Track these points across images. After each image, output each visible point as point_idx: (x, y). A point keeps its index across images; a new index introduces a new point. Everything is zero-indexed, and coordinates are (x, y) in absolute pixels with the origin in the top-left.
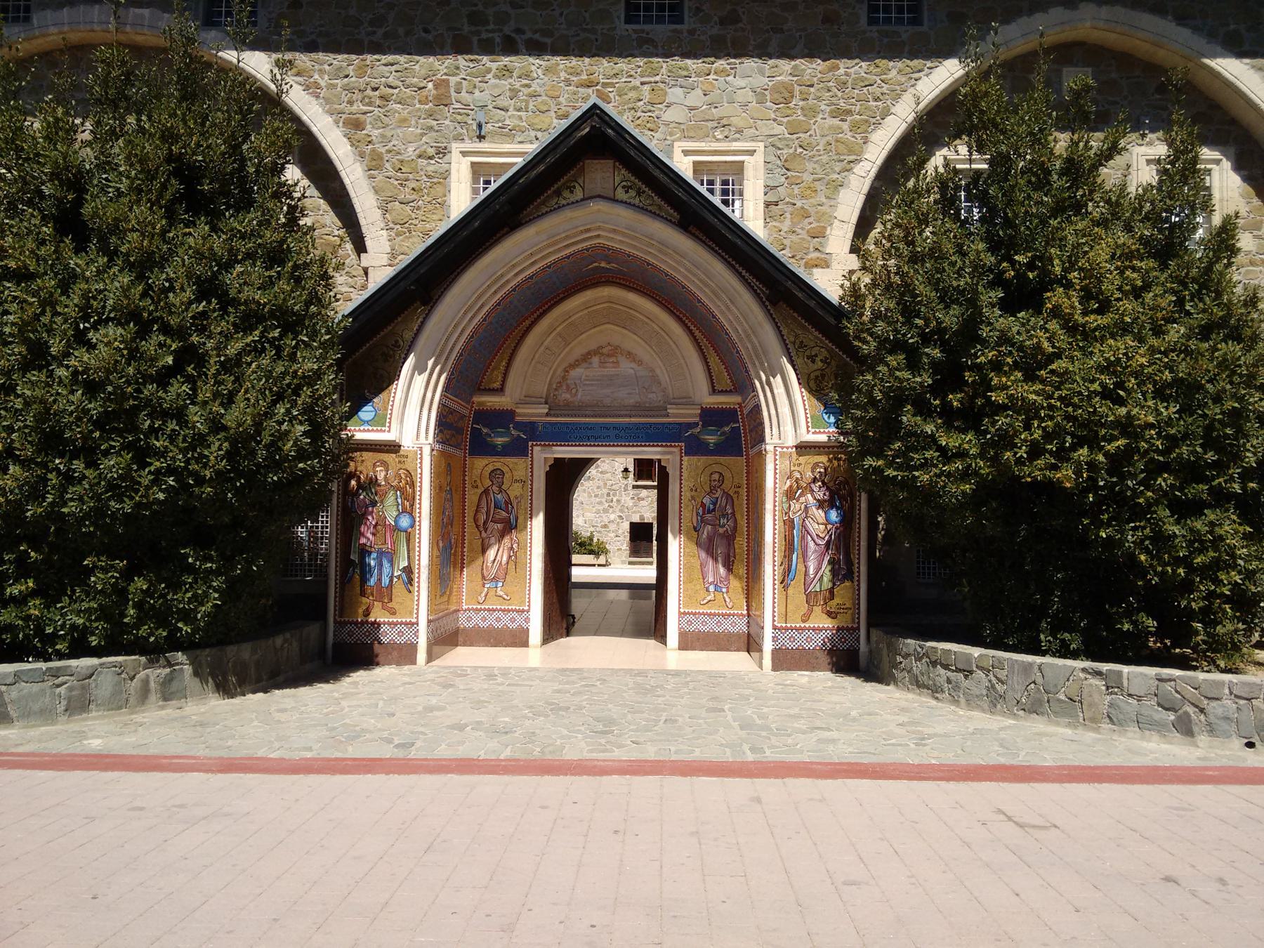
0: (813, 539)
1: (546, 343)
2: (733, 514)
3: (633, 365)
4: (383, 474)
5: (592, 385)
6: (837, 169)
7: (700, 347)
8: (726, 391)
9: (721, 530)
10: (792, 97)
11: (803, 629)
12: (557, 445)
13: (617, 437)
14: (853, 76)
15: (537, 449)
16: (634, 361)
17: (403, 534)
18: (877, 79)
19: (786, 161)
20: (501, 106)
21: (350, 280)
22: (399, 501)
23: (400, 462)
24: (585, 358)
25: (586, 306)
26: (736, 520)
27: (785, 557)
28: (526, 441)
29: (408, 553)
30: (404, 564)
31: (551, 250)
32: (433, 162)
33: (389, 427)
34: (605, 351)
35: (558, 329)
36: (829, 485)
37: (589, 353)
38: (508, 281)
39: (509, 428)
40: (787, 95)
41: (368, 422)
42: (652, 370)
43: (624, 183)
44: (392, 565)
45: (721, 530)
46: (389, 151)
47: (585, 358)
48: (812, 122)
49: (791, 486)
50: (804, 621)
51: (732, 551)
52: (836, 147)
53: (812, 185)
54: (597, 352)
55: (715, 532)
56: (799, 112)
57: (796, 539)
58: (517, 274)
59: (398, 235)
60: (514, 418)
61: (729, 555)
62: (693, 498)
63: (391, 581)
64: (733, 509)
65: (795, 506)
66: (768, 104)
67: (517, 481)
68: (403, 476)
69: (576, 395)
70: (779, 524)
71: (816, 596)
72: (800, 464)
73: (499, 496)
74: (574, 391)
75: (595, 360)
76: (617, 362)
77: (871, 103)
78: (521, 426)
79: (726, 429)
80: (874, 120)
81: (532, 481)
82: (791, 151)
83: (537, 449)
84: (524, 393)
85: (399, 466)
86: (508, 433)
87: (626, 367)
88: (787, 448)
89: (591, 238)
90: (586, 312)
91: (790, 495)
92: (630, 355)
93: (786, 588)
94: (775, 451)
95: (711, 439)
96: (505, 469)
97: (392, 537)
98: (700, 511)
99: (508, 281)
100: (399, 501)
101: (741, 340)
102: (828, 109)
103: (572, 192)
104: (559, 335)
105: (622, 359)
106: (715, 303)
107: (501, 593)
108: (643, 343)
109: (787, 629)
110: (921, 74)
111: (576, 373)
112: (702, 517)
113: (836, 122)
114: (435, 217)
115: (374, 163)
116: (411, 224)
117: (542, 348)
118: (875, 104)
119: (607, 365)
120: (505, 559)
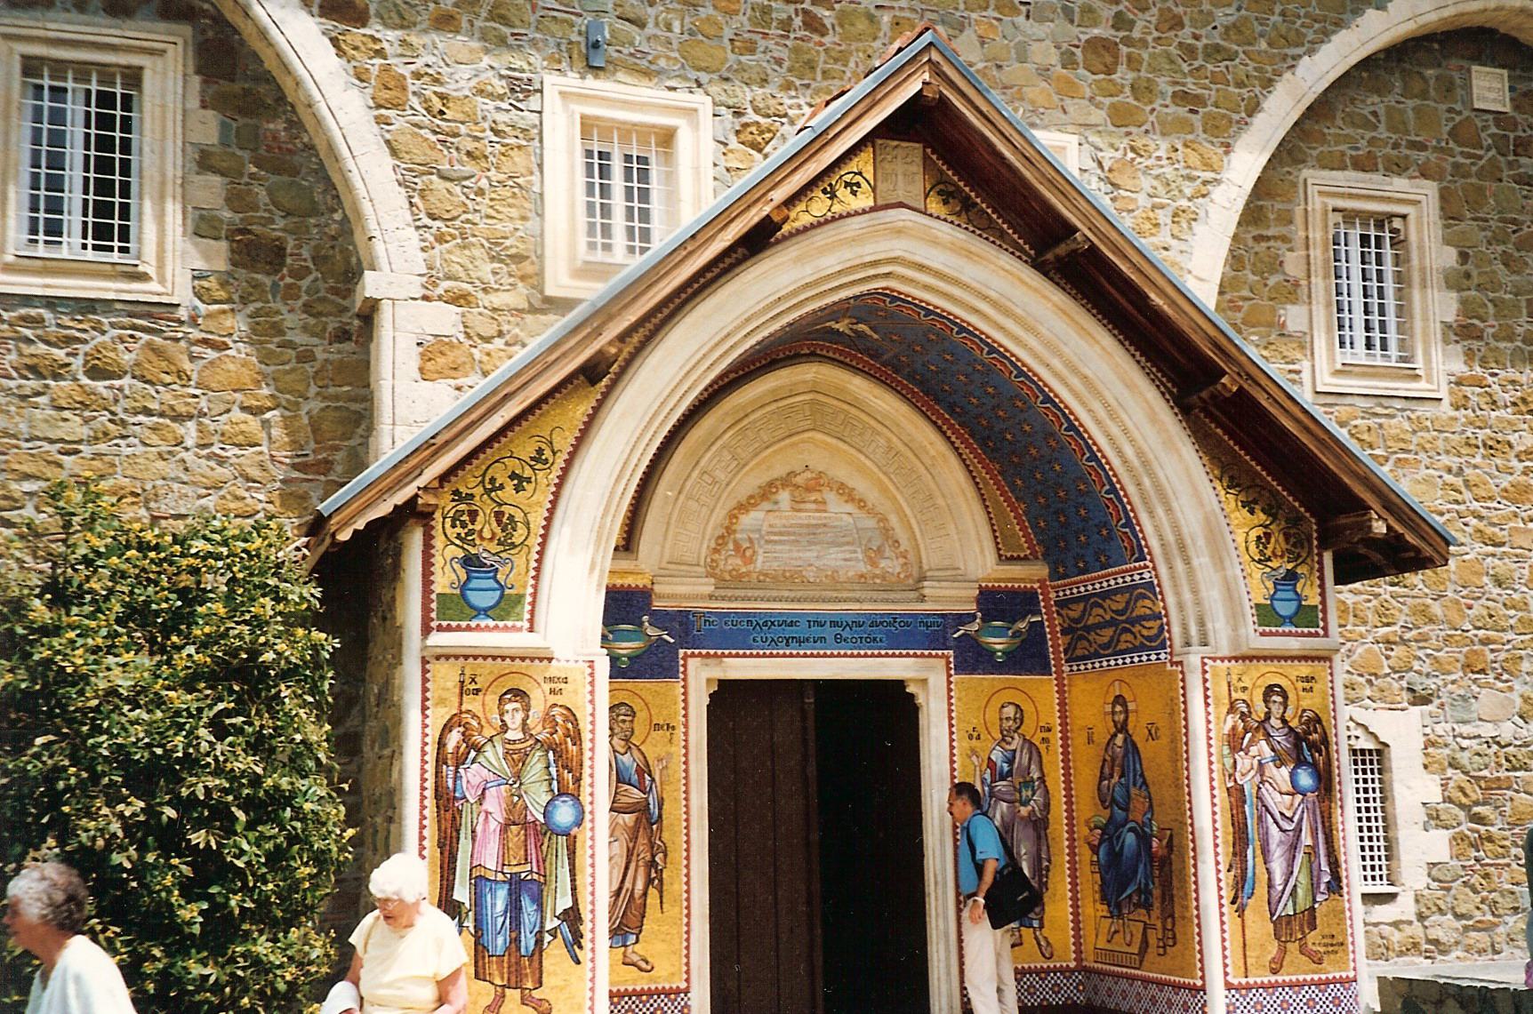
0: (1276, 822)
1: (703, 463)
2: (1042, 779)
3: (849, 508)
4: (520, 716)
5: (780, 542)
6: (1188, 192)
9: (1024, 811)
10: (1116, 63)
11: (1274, 986)
12: (730, 656)
13: (839, 639)
14: (1205, 41)
15: (693, 664)
16: (853, 500)
17: (562, 840)
18: (1240, 49)
19: (1110, 170)
20: (631, 16)
21: (312, 321)
22: (553, 770)
23: (552, 692)
24: (766, 493)
26: (1047, 792)
27: (1235, 854)
28: (673, 650)
29: (573, 880)
30: (565, 903)
31: (809, 294)
32: (505, 106)
33: (531, 621)
34: (799, 480)
36: (1295, 723)
37: (771, 484)
39: (641, 624)
40: (1109, 59)
41: (486, 612)
42: (884, 519)
43: (942, 187)
44: (541, 908)
45: (1024, 811)
46: (417, 75)
47: (766, 493)
48: (1148, 108)
49: (1234, 728)
50: (1275, 972)
51: (1044, 848)
52: (1186, 155)
53: (1151, 215)
54: (786, 481)
55: (1014, 814)
56: (1127, 90)
57: (1249, 821)
59: (440, 239)
60: (650, 604)
61: (1040, 859)
62: (974, 751)
63: (539, 941)
64: (1041, 770)
65: (1244, 762)
66: (1081, 71)
67: (658, 727)
68: (559, 720)
69: (751, 561)
70: (1221, 795)
71: (1288, 923)
72: (1244, 689)
73: (626, 759)
74: (748, 553)
75: (784, 496)
77: (1231, 89)
78: (661, 619)
79: (1022, 625)
80: (1236, 117)
81: (686, 726)
82: (1119, 155)
83: (693, 664)
84: (667, 557)
85: (553, 699)
86: (640, 633)
87: (838, 509)
88: (1222, 660)
90: (774, 406)
91: (1235, 743)
93: (1241, 912)
94: (1204, 664)
95: (998, 644)
96: (637, 705)
97: (539, 847)
98: (988, 776)
100: (553, 770)
101: (1130, 470)
102: (1170, 90)
103: (854, 193)
105: (831, 497)
106: (1083, 404)
107: (635, 958)
109: (1249, 988)
110: (1299, 51)
111: (749, 520)
112: (991, 788)
113: (1182, 111)
114: (514, 213)
115: (387, 94)
116: (468, 221)
118: (1237, 91)
120: (640, 886)
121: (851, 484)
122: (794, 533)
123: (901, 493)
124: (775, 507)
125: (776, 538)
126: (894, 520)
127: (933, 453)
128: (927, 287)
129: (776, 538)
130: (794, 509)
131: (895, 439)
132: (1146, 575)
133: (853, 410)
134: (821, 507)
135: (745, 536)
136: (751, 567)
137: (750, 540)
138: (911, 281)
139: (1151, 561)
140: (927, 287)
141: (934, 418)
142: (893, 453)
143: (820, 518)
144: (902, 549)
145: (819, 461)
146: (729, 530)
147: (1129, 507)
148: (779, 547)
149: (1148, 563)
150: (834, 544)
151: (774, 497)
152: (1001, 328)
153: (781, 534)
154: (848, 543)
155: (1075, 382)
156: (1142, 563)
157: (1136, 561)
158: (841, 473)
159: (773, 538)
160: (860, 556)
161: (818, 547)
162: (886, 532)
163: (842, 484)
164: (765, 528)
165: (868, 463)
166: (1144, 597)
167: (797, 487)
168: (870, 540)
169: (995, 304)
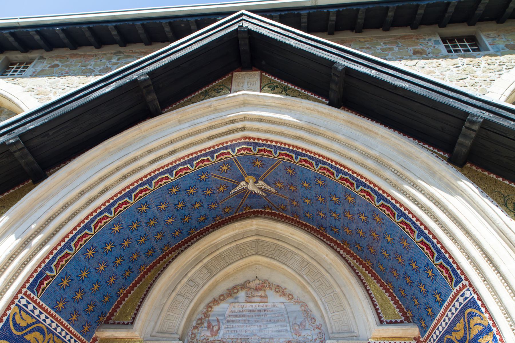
1: (190, 275)
3: (283, 299)
5: (237, 321)
7: (357, 274)
8: (396, 322)
16: (284, 295)
24: (232, 292)
25: (234, 239)
35: (205, 261)
37: (234, 288)
38: (142, 168)
42: (304, 305)
47: (232, 292)
54: (243, 286)
58: (152, 162)
69: (217, 333)
75: (242, 295)
76: (266, 296)
84: (157, 328)
89: (236, 130)
90: (234, 244)
92: (279, 290)
99: (142, 168)
104: (205, 266)
105: (270, 293)
106: (380, 176)
108: (294, 273)
111: (217, 309)
117: (185, 280)
119: (256, 299)
121: (283, 285)
122: (246, 316)
123: (311, 286)
124: (236, 301)
125: (234, 319)
126: (311, 305)
127: (329, 261)
128: (267, 131)
129: (234, 319)
130: (247, 302)
131: (305, 256)
132: (467, 294)
133: (280, 243)
134: (264, 299)
135: (215, 318)
136: (216, 338)
137: (218, 321)
138: (258, 130)
139: (467, 279)
140: (267, 131)
141: (322, 238)
142: (305, 263)
143: (263, 306)
144: (317, 323)
145: (264, 274)
146: (206, 315)
147: (435, 241)
148: (235, 325)
149: (467, 283)
150: (270, 321)
151: (235, 295)
152: (316, 144)
153: (237, 316)
154: (281, 321)
155: (369, 163)
156: (460, 285)
157: (456, 285)
158: (276, 279)
159: (232, 319)
160: (289, 329)
161: (261, 324)
162: (307, 312)
163: (278, 286)
164: (228, 313)
165: (289, 270)
166: (471, 316)
167: (250, 289)
168: (295, 318)
169: (309, 131)
